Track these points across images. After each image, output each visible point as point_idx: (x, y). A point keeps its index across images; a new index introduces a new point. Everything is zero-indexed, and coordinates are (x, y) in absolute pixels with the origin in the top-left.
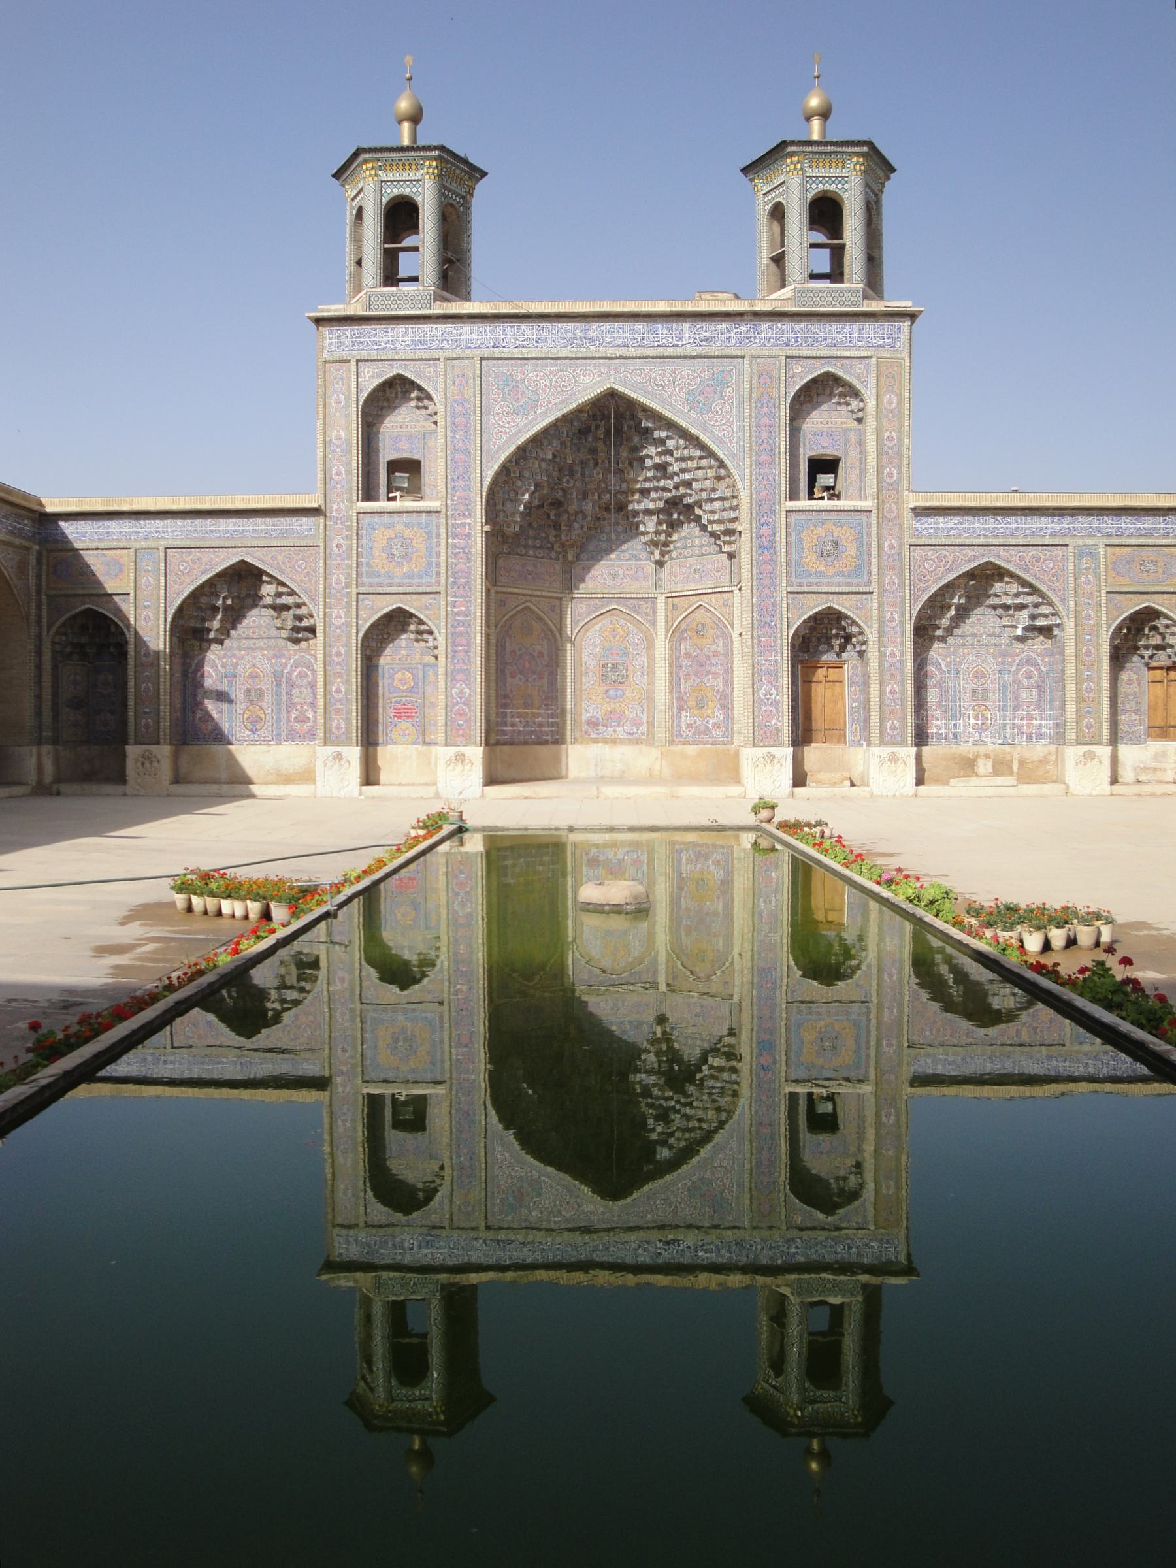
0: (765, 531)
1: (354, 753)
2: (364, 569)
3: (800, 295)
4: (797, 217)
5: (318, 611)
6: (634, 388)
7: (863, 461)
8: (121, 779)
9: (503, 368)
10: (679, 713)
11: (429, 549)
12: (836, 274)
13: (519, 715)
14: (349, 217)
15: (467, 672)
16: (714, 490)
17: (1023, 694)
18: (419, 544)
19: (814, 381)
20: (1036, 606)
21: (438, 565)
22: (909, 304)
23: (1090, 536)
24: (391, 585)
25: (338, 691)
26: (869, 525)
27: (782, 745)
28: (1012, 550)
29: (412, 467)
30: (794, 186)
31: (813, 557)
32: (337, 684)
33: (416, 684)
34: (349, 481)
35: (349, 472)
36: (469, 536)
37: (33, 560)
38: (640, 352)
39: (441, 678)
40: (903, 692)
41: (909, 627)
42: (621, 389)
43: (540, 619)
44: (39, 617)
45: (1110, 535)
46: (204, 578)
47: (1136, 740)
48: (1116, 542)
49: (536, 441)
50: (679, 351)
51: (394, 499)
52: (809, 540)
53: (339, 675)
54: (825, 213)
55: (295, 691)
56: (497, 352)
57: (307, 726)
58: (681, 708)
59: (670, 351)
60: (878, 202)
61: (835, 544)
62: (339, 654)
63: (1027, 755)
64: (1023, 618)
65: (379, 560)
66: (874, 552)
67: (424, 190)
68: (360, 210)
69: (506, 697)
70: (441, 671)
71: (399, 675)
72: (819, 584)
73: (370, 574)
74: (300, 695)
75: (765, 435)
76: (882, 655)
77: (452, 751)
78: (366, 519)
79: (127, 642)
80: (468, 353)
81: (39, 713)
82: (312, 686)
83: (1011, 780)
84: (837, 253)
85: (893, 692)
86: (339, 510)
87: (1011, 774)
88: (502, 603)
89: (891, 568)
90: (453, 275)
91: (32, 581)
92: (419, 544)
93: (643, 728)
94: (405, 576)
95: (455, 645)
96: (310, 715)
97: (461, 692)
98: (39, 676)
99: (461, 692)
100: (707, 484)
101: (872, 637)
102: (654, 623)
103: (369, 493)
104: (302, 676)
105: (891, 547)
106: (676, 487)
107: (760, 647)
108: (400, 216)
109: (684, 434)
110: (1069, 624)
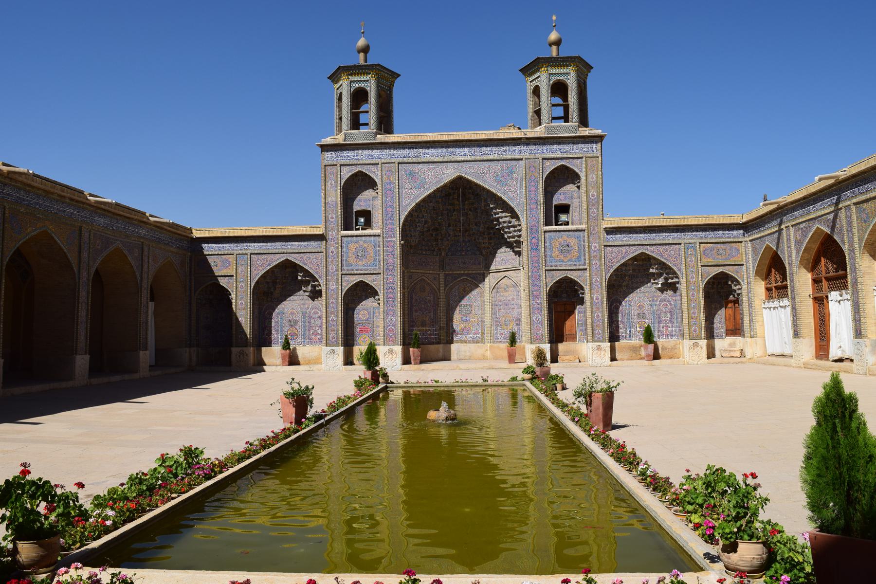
0: (534, 241)
1: (340, 350)
2: (344, 263)
3: (547, 128)
4: (545, 92)
5: (322, 282)
6: (470, 174)
7: (581, 206)
9: (409, 167)
10: (496, 329)
11: (375, 252)
12: (566, 119)
13: (419, 330)
14: (335, 98)
15: (394, 311)
16: (510, 222)
17: (663, 315)
18: (370, 250)
19: (556, 169)
21: (379, 260)
22: (600, 131)
23: (691, 238)
24: (357, 270)
25: (333, 320)
26: (584, 237)
27: (545, 343)
28: (654, 247)
29: (367, 215)
30: (543, 79)
31: (557, 253)
32: (332, 317)
33: (370, 318)
34: (337, 221)
35: (337, 217)
36: (393, 246)
38: (473, 158)
39: (382, 313)
40: (603, 316)
41: (604, 285)
42: (464, 176)
43: (429, 284)
45: (701, 238)
46: (269, 268)
47: (721, 337)
48: (705, 241)
49: (423, 200)
50: (491, 157)
51: (358, 229)
52: (555, 244)
53: (333, 313)
54: (559, 89)
55: (312, 321)
56: (406, 160)
57: (318, 337)
58: (498, 325)
59: (487, 157)
60: (585, 83)
61: (568, 246)
62: (333, 303)
63: (666, 345)
64: (661, 280)
65: (351, 258)
66: (587, 250)
67: (370, 84)
68: (341, 94)
69: (413, 322)
70: (382, 310)
71: (361, 313)
72: (561, 265)
73: (349, 265)
74: (315, 322)
75: (533, 195)
76: (592, 298)
78: (345, 239)
80: (392, 160)
82: (320, 318)
84: (566, 108)
86: (332, 235)
88: (410, 277)
89: (595, 257)
90: (385, 124)
92: (370, 250)
94: (364, 265)
96: (319, 332)
97: (391, 320)
99: (391, 320)
100: (507, 219)
103: (347, 226)
104: (315, 313)
105: (595, 247)
106: (493, 221)
107: (532, 296)
108: (359, 97)
110: (683, 281)
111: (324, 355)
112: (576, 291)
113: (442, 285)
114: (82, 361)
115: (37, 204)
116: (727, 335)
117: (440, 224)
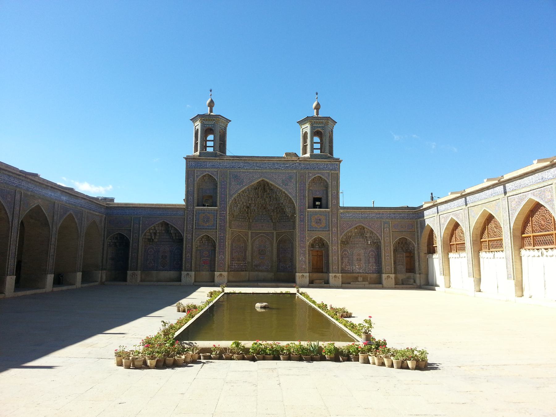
0: (302, 216)
8: (125, 280)
17: (371, 259)
20: (374, 237)
34: (193, 201)
35: (193, 199)
37: (103, 219)
41: (339, 242)
44: (104, 235)
60: (332, 131)
61: (320, 220)
77: (219, 273)
79: (129, 242)
81: (102, 262)
82: (181, 255)
83: (367, 283)
85: (335, 259)
87: (368, 281)
88: (232, 233)
91: (103, 224)
93: (270, 267)
95: (220, 245)
98: (103, 251)
101: (330, 245)
102: (273, 240)
108: (207, 131)
109: (281, 191)
111: (183, 276)
112: (323, 244)
113: (250, 238)
114: (50, 278)
115: (35, 190)
116: (406, 272)
117: (250, 204)
